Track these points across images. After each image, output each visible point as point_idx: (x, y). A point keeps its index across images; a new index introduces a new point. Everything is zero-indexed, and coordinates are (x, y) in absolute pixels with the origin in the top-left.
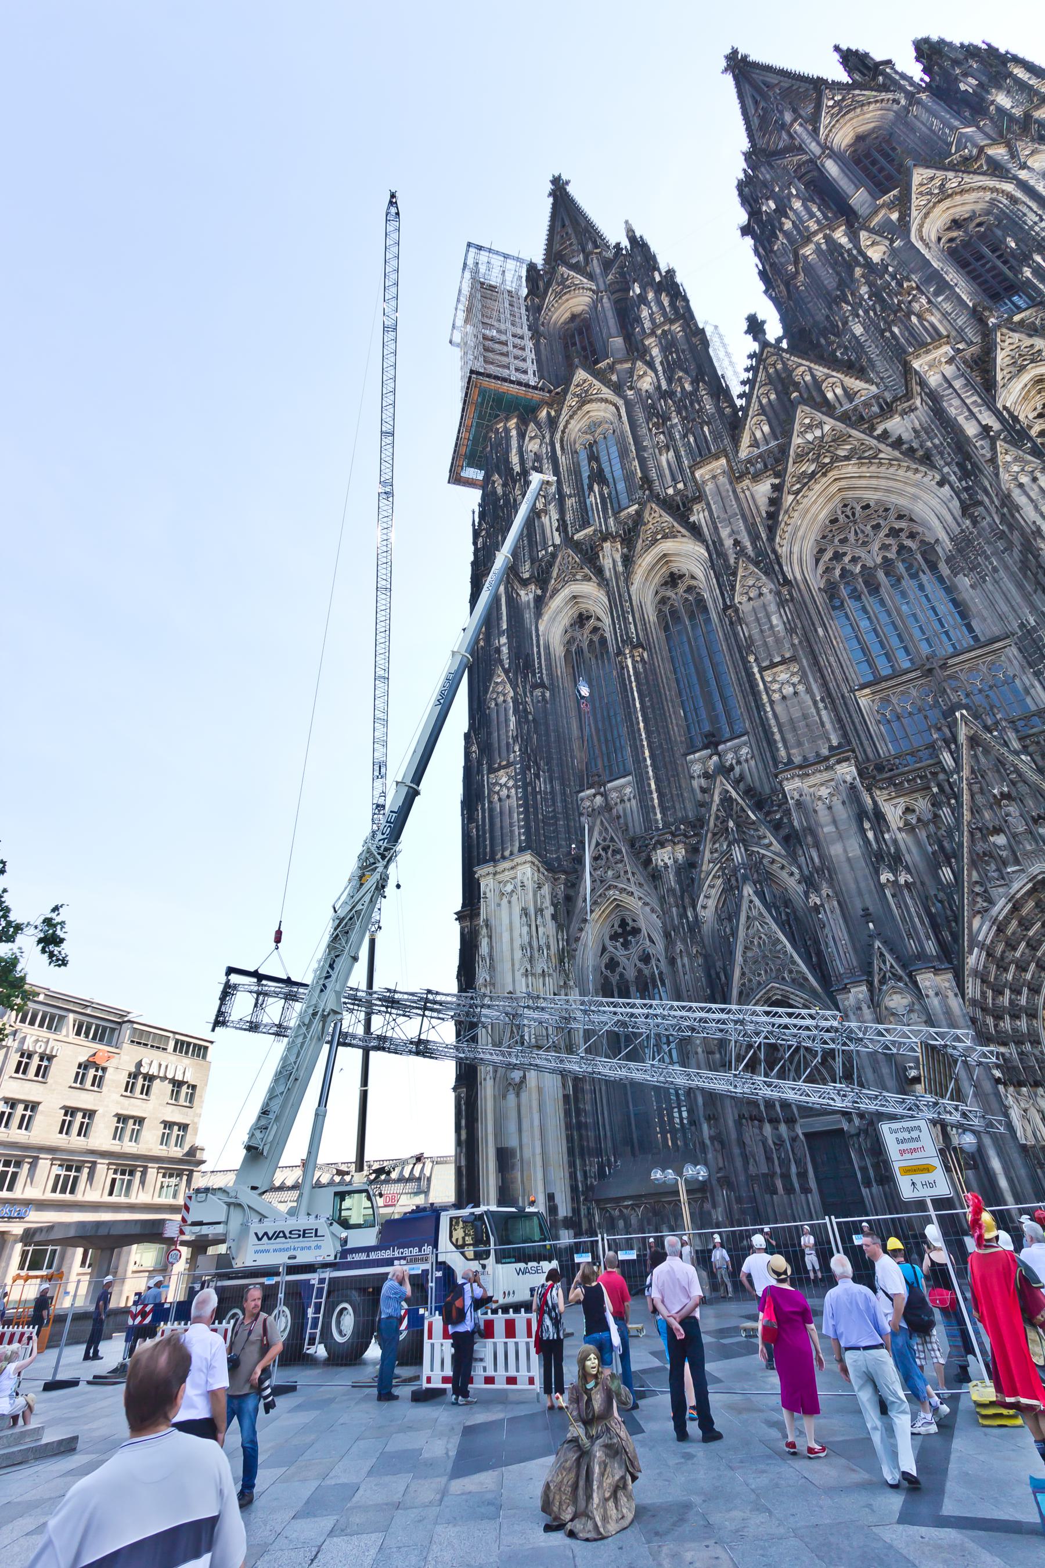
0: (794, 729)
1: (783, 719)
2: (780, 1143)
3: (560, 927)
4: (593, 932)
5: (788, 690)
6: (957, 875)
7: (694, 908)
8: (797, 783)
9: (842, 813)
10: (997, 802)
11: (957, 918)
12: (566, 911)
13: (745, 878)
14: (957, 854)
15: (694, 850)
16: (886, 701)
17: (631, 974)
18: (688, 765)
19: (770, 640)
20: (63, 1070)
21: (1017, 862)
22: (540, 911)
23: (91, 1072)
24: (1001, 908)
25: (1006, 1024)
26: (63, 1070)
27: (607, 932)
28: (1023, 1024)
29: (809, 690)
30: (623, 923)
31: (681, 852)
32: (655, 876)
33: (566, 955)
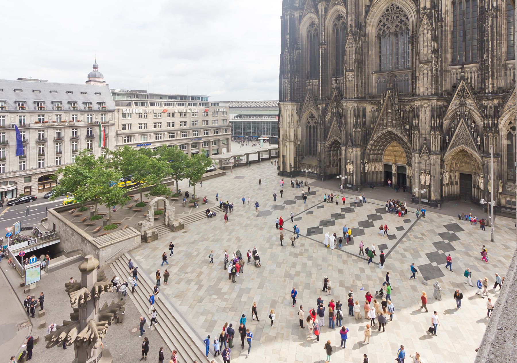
0: (349, 90)
1: (348, 86)
2: (334, 160)
3: (298, 115)
4: (305, 115)
5: (350, 79)
6: (374, 127)
7: (324, 118)
8: (345, 104)
9: (352, 112)
10: (387, 114)
11: (371, 134)
12: (300, 112)
13: (335, 116)
14: (376, 122)
15: (327, 105)
16: (379, 78)
17: (312, 126)
18: (331, 81)
19: (351, 62)
21: (386, 127)
22: (292, 115)
24: (380, 134)
26: (200, 114)
27: (309, 116)
29: (355, 81)
30: (312, 115)
31: (324, 106)
32: (318, 109)
33: (299, 121)
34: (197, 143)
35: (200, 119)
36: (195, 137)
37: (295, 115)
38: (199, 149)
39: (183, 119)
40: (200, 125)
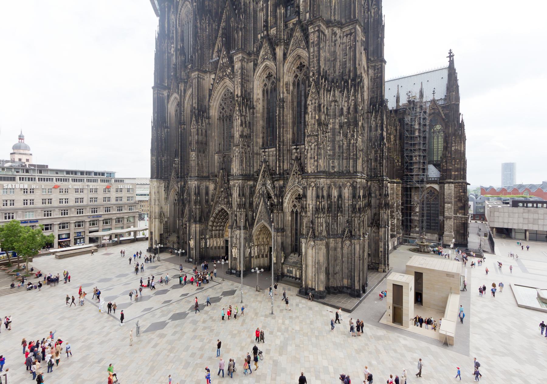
3: (165, 193)
20: (101, 191)
23: (107, 189)
25: (218, 228)
26: (101, 191)
28: (221, 228)
34: (96, 221)
35: (100, 196)
36: (93, 214)
37: (163, 192)
38: (98, 227)
39: (79, 195)
40: (100, 201)
